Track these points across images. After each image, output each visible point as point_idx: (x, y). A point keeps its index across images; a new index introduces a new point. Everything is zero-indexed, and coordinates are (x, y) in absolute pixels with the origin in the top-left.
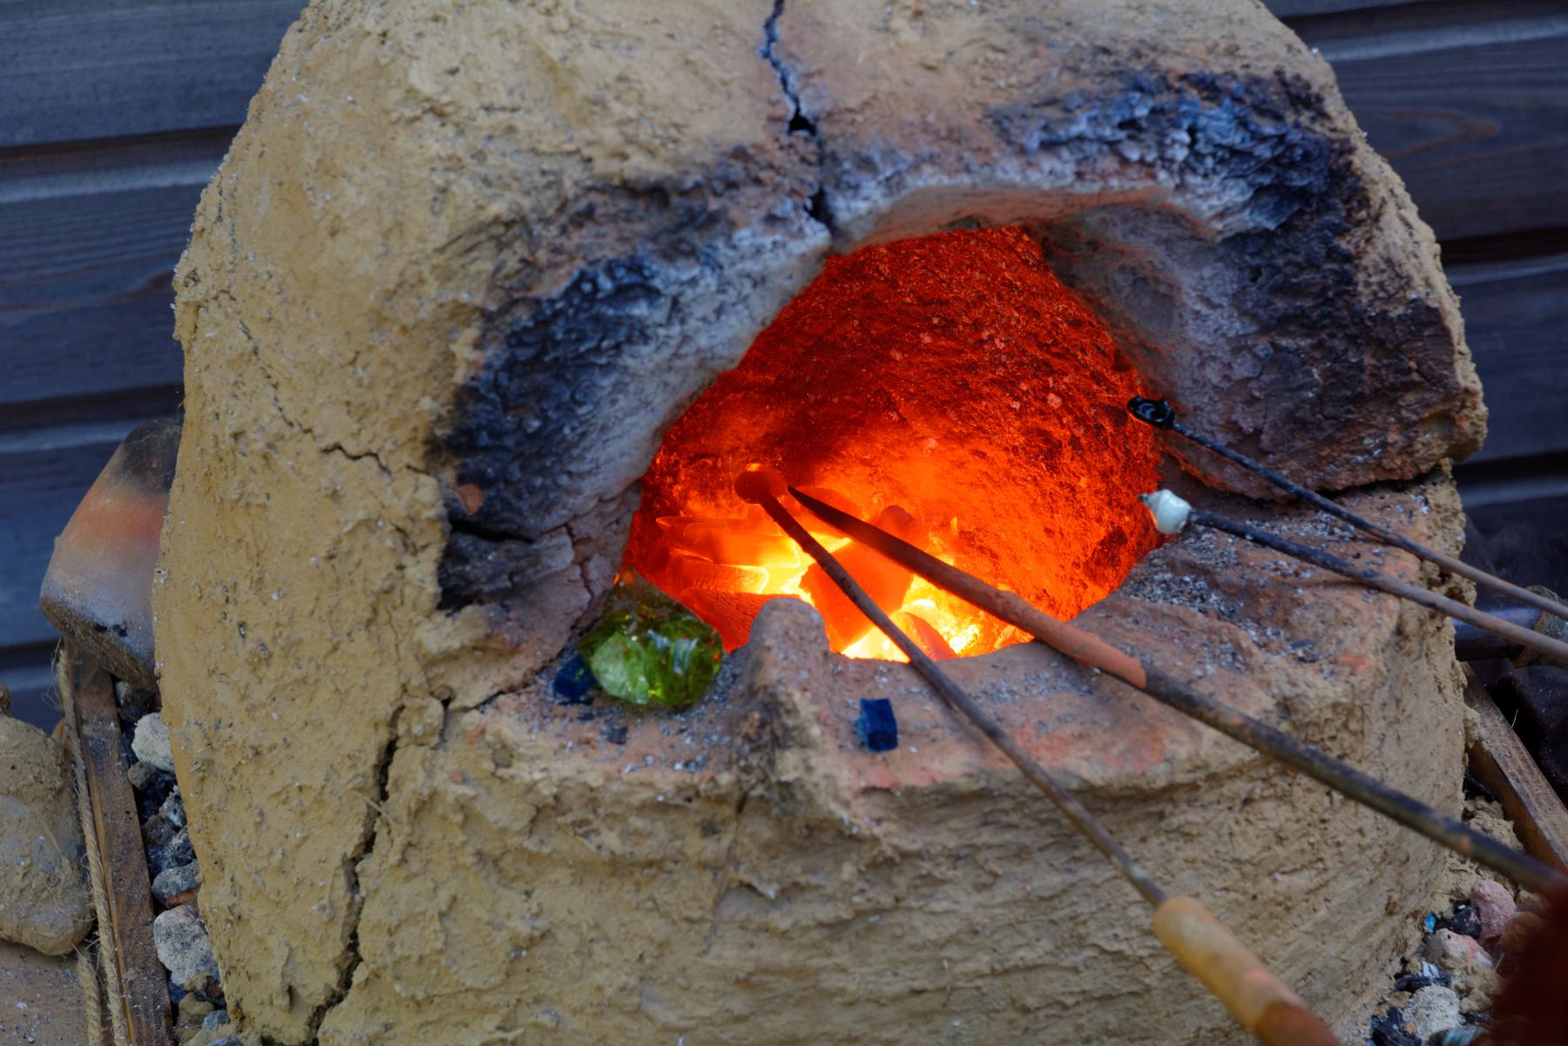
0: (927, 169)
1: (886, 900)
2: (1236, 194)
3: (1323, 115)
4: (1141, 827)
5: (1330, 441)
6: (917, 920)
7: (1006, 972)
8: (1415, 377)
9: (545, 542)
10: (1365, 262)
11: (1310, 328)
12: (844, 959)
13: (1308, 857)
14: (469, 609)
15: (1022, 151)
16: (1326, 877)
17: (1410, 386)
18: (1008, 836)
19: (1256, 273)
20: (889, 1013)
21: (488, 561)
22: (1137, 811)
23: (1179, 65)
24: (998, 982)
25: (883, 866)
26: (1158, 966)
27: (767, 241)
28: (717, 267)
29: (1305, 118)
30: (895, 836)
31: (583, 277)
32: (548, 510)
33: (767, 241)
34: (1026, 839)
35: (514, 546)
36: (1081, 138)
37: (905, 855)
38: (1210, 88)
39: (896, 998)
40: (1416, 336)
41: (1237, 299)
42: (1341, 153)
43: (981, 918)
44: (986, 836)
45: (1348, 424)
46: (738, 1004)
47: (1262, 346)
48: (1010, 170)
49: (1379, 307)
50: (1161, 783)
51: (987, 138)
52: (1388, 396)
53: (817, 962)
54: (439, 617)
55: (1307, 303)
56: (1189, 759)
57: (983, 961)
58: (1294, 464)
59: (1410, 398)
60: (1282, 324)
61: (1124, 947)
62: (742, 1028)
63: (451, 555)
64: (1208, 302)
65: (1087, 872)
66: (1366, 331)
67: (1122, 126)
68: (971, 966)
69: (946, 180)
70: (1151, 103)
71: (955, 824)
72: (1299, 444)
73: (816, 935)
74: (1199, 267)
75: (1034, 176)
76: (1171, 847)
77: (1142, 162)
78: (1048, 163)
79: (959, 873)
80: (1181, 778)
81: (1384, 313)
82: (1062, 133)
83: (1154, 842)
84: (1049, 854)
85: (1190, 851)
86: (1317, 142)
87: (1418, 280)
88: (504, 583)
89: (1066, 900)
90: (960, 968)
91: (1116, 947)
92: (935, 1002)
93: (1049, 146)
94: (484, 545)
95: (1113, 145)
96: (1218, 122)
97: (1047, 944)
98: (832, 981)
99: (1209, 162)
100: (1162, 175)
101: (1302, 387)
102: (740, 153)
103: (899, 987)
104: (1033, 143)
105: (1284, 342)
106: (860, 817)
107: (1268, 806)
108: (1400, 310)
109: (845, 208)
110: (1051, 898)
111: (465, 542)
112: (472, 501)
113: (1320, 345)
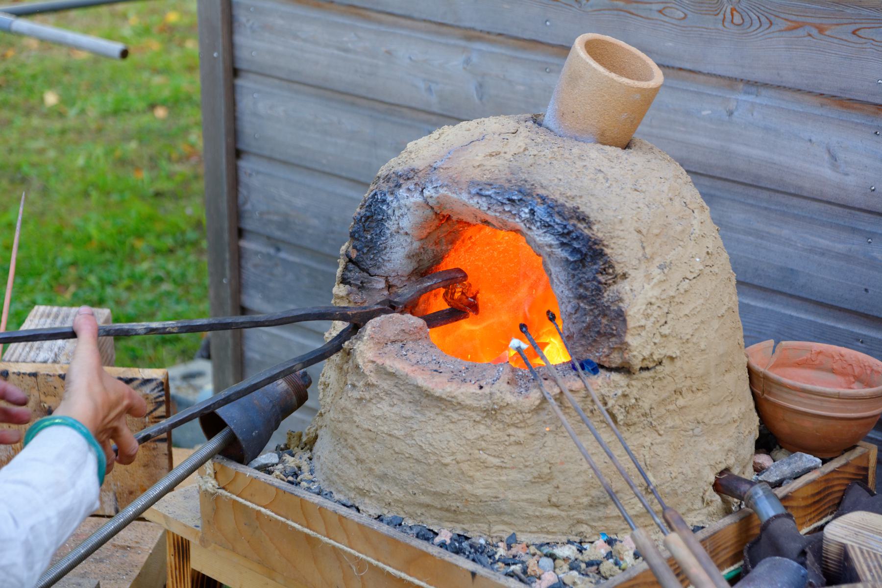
0: (445, 188)
1: (368, 397)
2: (549, 239)
3: (590, 228)
4: (438, 410)
5: (590, 344)
6: (374, 407)
7: (390, 435)
8: (615, 332)
9: (376, 278)
10: (611, 288)
11: (591, 303)
12: (358, 412)
13: (497, 454)
14: (347, 286)
15: (470, 193)
16: (504, 465)
17: (614, 336)
18: (401, 393)
19: (574, 276)
20: (364, 434)
21: (355, 274)
22: (435, 403)
23: (541, 192)
24: (389, 438)
25: (369, 385)
26: (434, 458)
27: (405, 195)
28: (398, 200)
29: (581, 226)
30: (373, 379)
31: (376, 194)
32: (379, 268)
33: (405, 195)
34: (405, 396)
35: (365, 274)
36: (490, 196)
37: (373, 385)
38: (543, 199)
39: (365, 430)
40: (617, 318)
41: (567, 283)
42: (596, 244)
43: (388, 414)
44: (395, 390)
45: (595, 341)
46: (341, 417)
47: (574, 302)
48: (464, 197)
49: (609, 304)
50: (437, 394)
51: (464, 187)
52: (610, 335)
53: (354, 410)
54: (342, 286)
55: (588, 293)
56: (450, 392)
57: (385, 429)
58: (580, 348)
59: (613, 339)
60: (581, 297)
61: (423, 445)
62: (340, 425)
63: (346, 268)
64: (558, 280)
65: (419, 416)
66: (604, 311)
67: (509, 200)
68: (382, 428)
69: (450, 194)
70: (520, 197)
71: (388, 382)
72: (583, 343)
73: (355, 401)
74: (555, 266)
75: (471, 201)
76: (446, 422)
77: (510, 211)
78: (476, 199)
79: (387, 399)
80: (444, 396)
81: (609, 306)
82: (483, 192)
83: (440, 418)
84: (411, 405)
85: (452, 426)
86: (581, 234)
87: (627, 301)
88: (358, 283)
89: (411, 421)
90: (380, 428)
91: (421, 444)
92: (373, 436)
93: (479, 194)
94: (357, 269)
95: (503, 204)
96: (540, 210)
97: (402, 433)
98: (356, 418)
99: (539, 224)
100: (517, 220)
101: (583, 322)
102: (413, 170)
103: (366, 427)
104: (473, 191)
105: (582, 305)
106: (367, 368)
107: (482, 427)
108: (616, 308)
109: (426, 193)
110: (405, 418)
111: (351, 266)
112: (354, 254)
113: (591, 310)
